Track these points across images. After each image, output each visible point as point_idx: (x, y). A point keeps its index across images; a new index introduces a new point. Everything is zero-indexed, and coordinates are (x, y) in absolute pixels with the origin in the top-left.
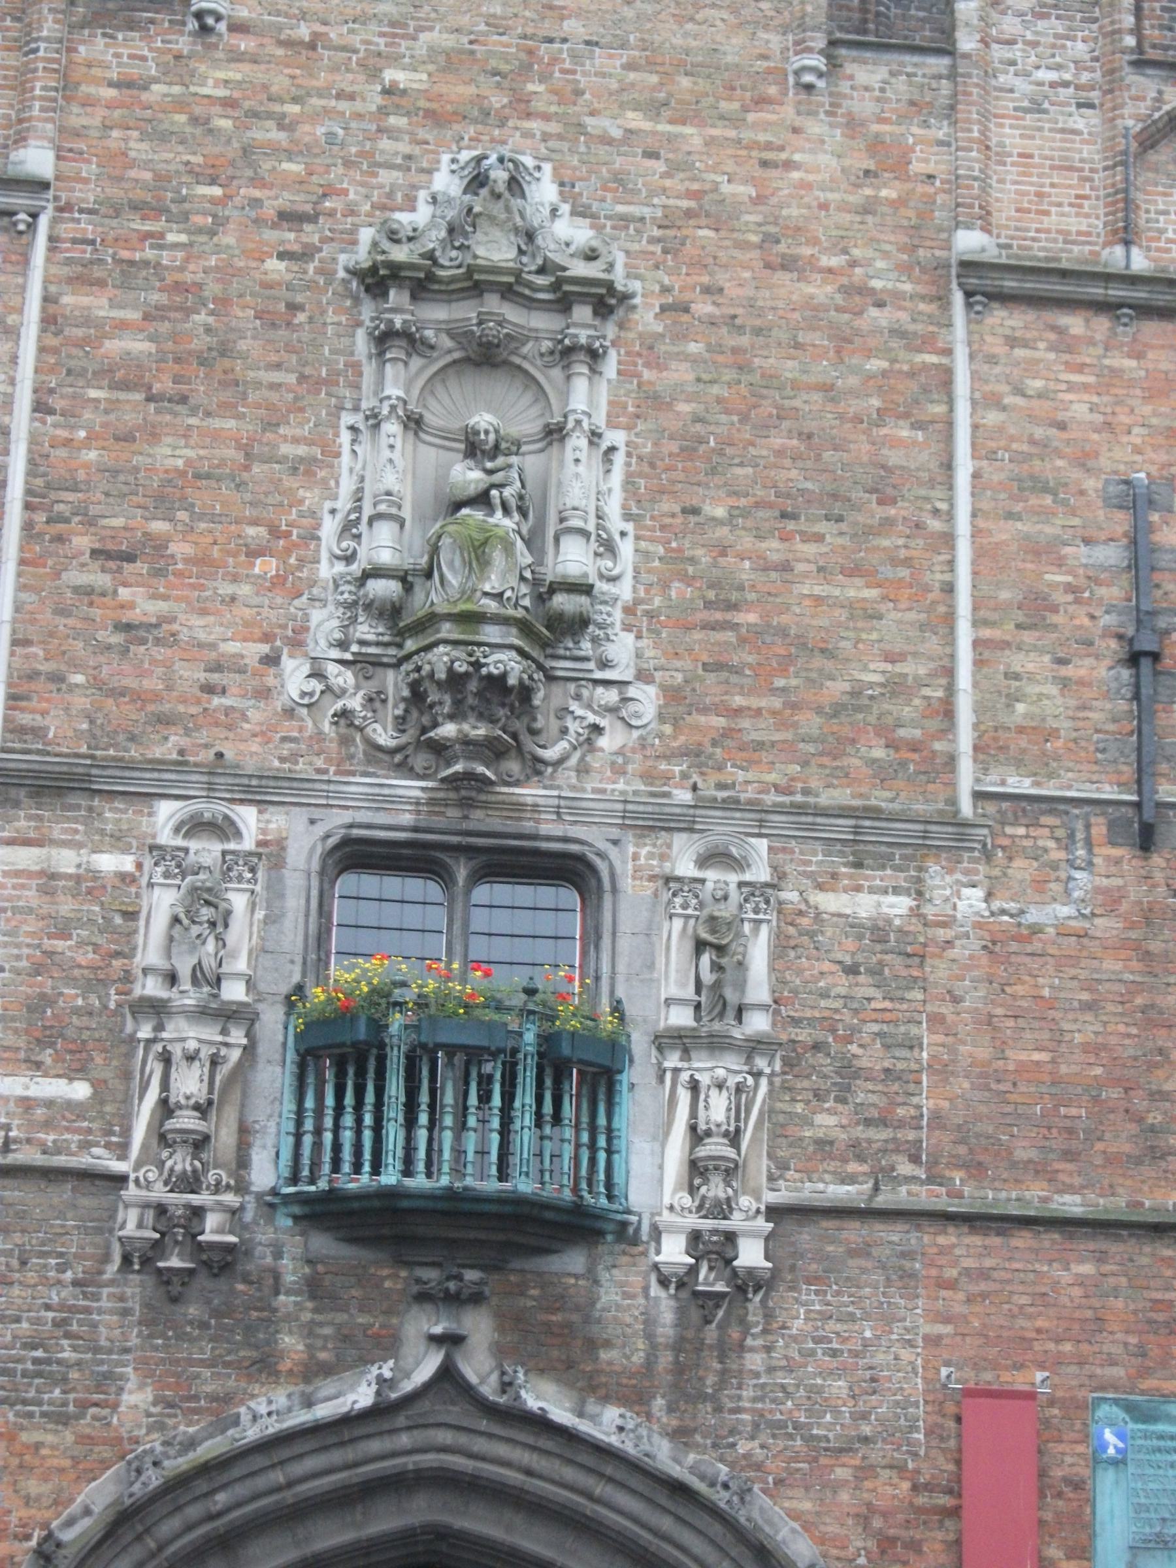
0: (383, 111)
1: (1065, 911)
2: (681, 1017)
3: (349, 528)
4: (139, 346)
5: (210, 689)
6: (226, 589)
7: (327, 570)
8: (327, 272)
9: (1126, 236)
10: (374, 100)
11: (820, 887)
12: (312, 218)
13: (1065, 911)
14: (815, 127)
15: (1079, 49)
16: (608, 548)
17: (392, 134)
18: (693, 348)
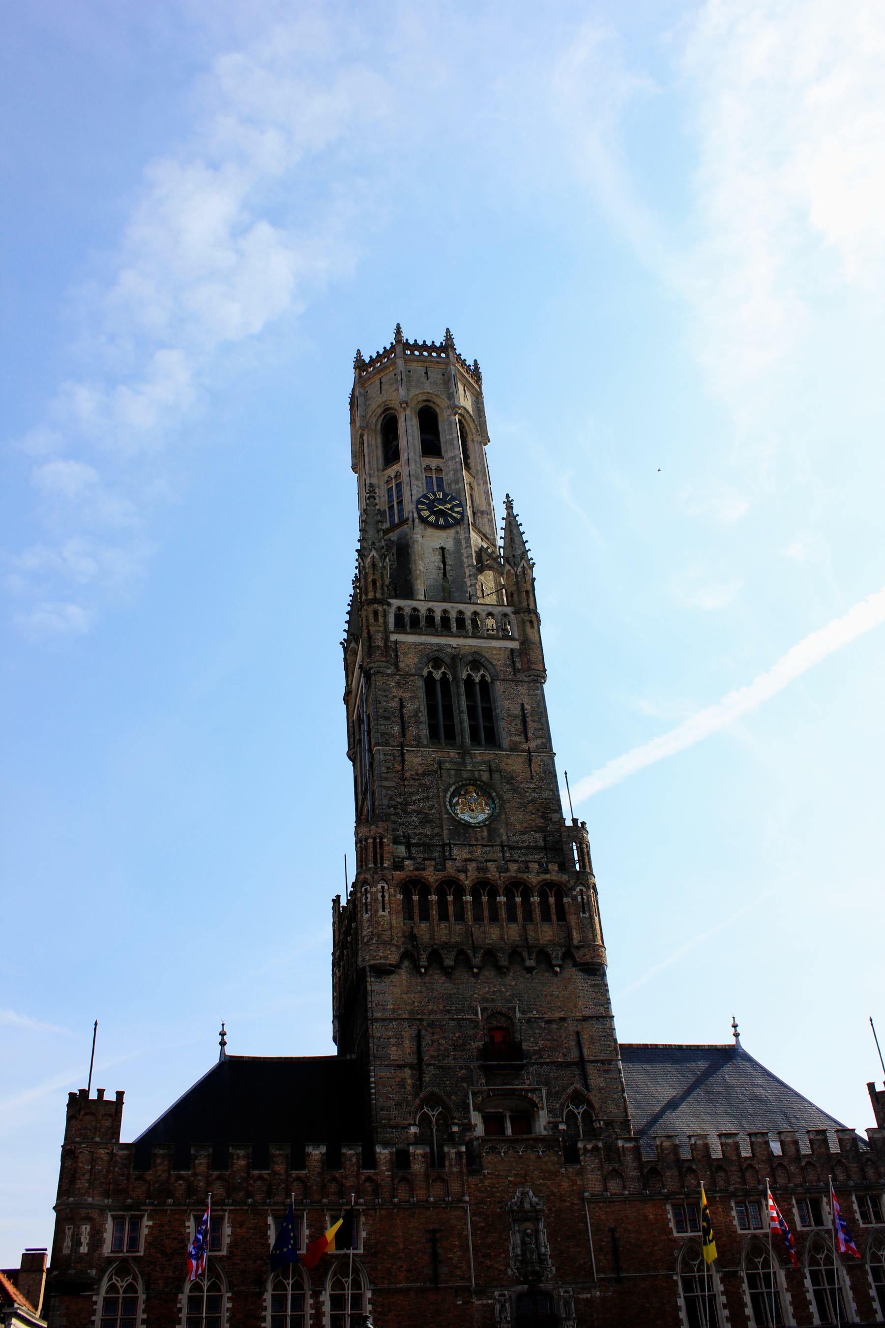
0: (509, 1184)
1: (610, 1294)
2: (564, 1316)
3: (513, 1249)
4: (483, 1224)
5: (499, 1275)
6: (499, 1259)
7: (511, 1255)
8: (505, 1209)
9: (606, 1190)
10: (507, 1183)
11: (579, 1294)
12: (502, 1202)
13: (610, 1294)
14: (564, 1179)
15: (597, 1161)
16: (546, 1247)
17: (511, 1187)
18: (553, 1215)
